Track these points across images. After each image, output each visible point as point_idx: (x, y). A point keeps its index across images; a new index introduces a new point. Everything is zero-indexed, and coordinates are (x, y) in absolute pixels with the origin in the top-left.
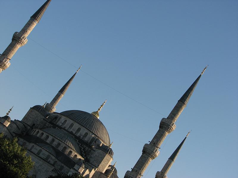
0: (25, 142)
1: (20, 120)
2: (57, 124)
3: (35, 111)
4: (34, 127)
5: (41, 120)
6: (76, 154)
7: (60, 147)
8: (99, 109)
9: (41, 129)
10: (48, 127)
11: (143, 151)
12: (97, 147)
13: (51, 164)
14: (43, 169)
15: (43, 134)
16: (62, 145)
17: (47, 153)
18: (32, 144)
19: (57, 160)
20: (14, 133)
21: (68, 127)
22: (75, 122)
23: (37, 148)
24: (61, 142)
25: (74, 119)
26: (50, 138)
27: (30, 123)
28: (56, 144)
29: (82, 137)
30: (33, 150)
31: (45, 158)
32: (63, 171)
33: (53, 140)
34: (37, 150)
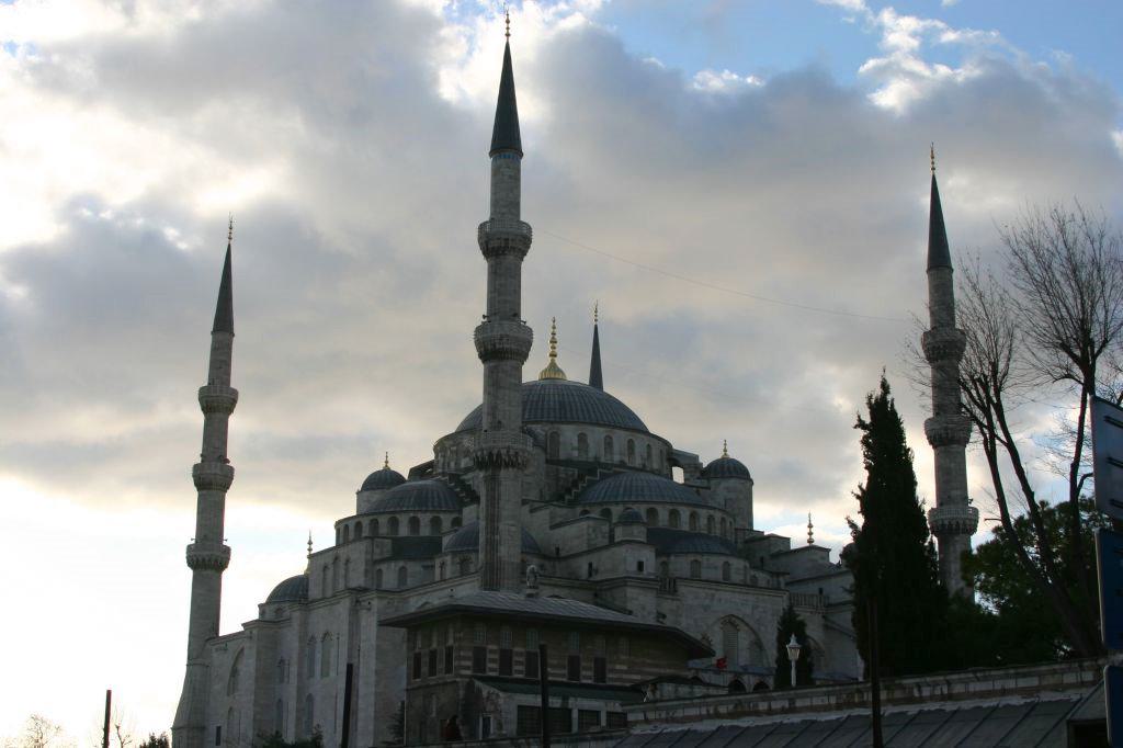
8: (553, 355)
14: (764, 612)
28: (705, 521)
30: (705, 574)
34: (716, 568)
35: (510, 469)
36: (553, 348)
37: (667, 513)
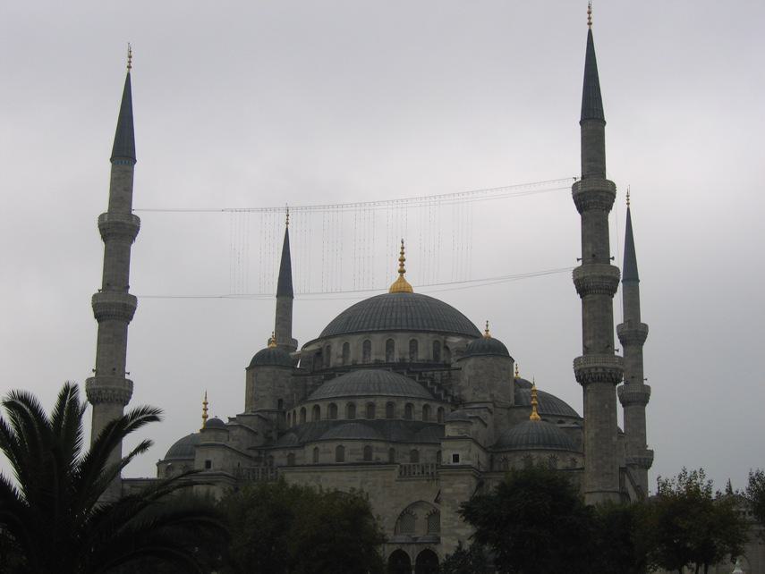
0: (291, 454)
1: (242, 411)
2: (331, 365)
3: (261, 369)
4: (284, 408)
5: (290, 379)
6: (424, 403)
7: (376, 410)
8: (402, 272)
9: (304, 400)
10: (315, 387)
11: (579, 291)
12: (459, 357)
13: (386, 464)
15: (317, 408)
16: (378, 405)
17: (360, 445)
18: (310, 449)
19: (391, 446)
20: (249, 449)
21: (361, 355)
22: (370, 332)
23: (328, 452)
24: (372, 400)
25: (374, 327)
26: (342, 407)
27: (269, 405)
29: (408, 357)
30: (322, 459)
31: (362, 457)
32: (422, 461)
33: (352, 407)
34: (330, 452)
35: (101, 404)
36: (402, 265)
37: (326, 408)
